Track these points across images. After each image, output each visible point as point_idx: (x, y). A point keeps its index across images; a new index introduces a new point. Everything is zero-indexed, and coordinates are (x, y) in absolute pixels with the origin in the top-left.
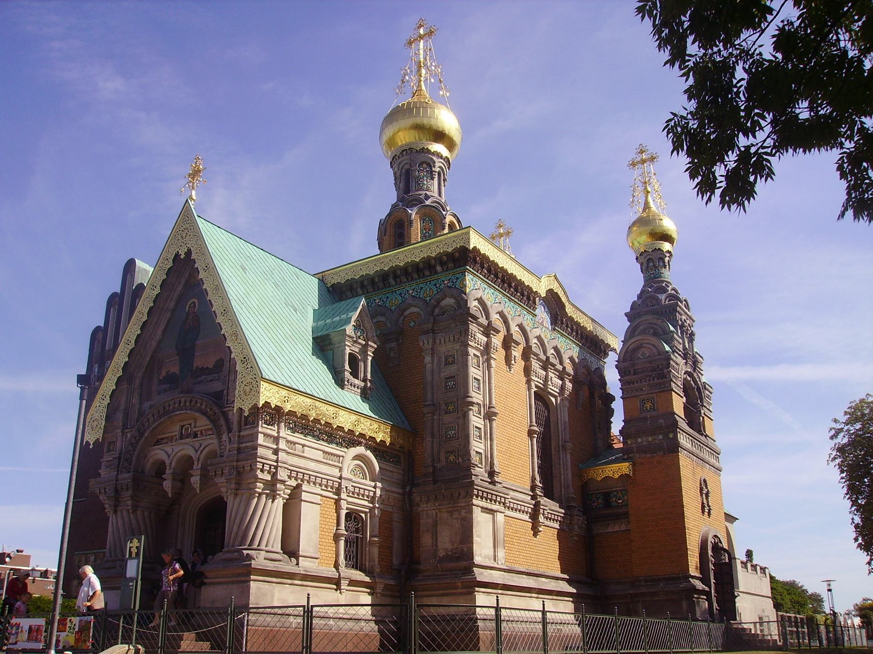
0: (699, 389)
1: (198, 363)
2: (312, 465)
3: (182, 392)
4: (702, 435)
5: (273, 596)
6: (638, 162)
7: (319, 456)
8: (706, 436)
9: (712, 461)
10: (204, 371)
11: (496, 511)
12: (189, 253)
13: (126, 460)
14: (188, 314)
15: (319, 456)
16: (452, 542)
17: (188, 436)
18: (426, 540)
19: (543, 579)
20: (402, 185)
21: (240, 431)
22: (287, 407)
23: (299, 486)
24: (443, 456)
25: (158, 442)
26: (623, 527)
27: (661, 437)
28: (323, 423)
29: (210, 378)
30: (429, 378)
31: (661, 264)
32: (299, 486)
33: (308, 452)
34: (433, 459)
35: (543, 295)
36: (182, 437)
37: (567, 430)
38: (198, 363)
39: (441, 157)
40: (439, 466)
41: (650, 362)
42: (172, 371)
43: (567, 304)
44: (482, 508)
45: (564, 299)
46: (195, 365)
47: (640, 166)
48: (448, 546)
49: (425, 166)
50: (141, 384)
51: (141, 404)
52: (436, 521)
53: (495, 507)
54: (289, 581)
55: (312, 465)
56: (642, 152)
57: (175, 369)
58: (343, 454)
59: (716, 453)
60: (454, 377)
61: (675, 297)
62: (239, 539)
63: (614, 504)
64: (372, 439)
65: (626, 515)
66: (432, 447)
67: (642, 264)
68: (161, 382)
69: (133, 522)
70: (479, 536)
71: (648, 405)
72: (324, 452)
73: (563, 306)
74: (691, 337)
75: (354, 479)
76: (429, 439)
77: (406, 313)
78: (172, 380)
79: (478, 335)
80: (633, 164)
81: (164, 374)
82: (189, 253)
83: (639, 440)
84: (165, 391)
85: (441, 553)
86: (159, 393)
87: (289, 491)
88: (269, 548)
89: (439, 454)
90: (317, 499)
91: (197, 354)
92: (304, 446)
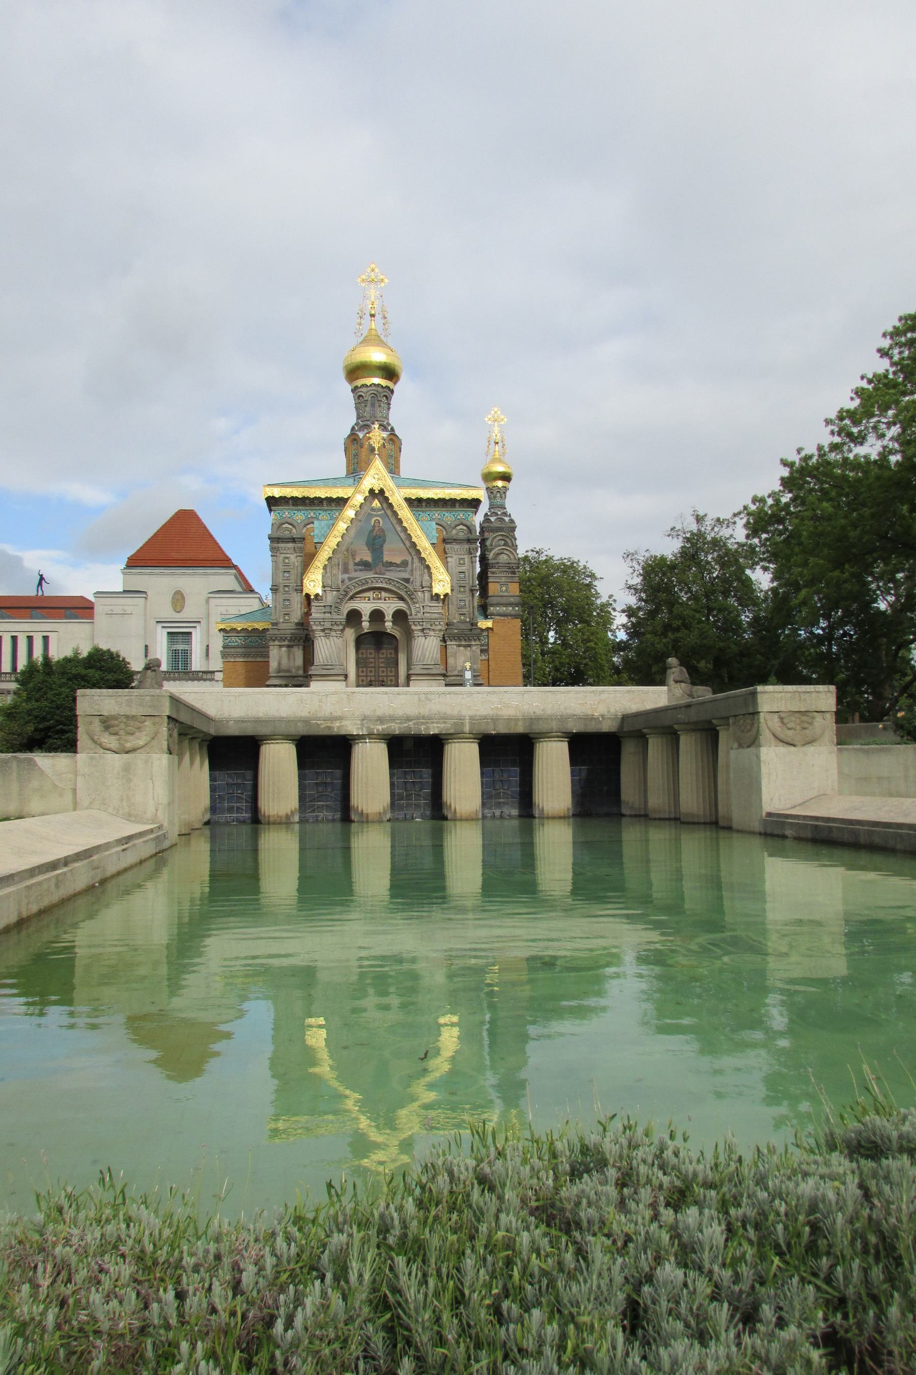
1: (386, 558)
3: (376, 573)
10: (391, 564)
12: (382, 491)
14: (374, 526)
17: (380, 599)
18: (451, 661)
36: (374, 599)
38: (386, 558)
42: (365, 559)
46: (385, 560)
57: (368, 557)
61: (512, 521)
68: (356, 564)
71: (504, 588)
78: (365, 565)
81: (357, 560)
82: (382, 491)
84: (361, 570)
86: (356, 571)
91: (385, 553)
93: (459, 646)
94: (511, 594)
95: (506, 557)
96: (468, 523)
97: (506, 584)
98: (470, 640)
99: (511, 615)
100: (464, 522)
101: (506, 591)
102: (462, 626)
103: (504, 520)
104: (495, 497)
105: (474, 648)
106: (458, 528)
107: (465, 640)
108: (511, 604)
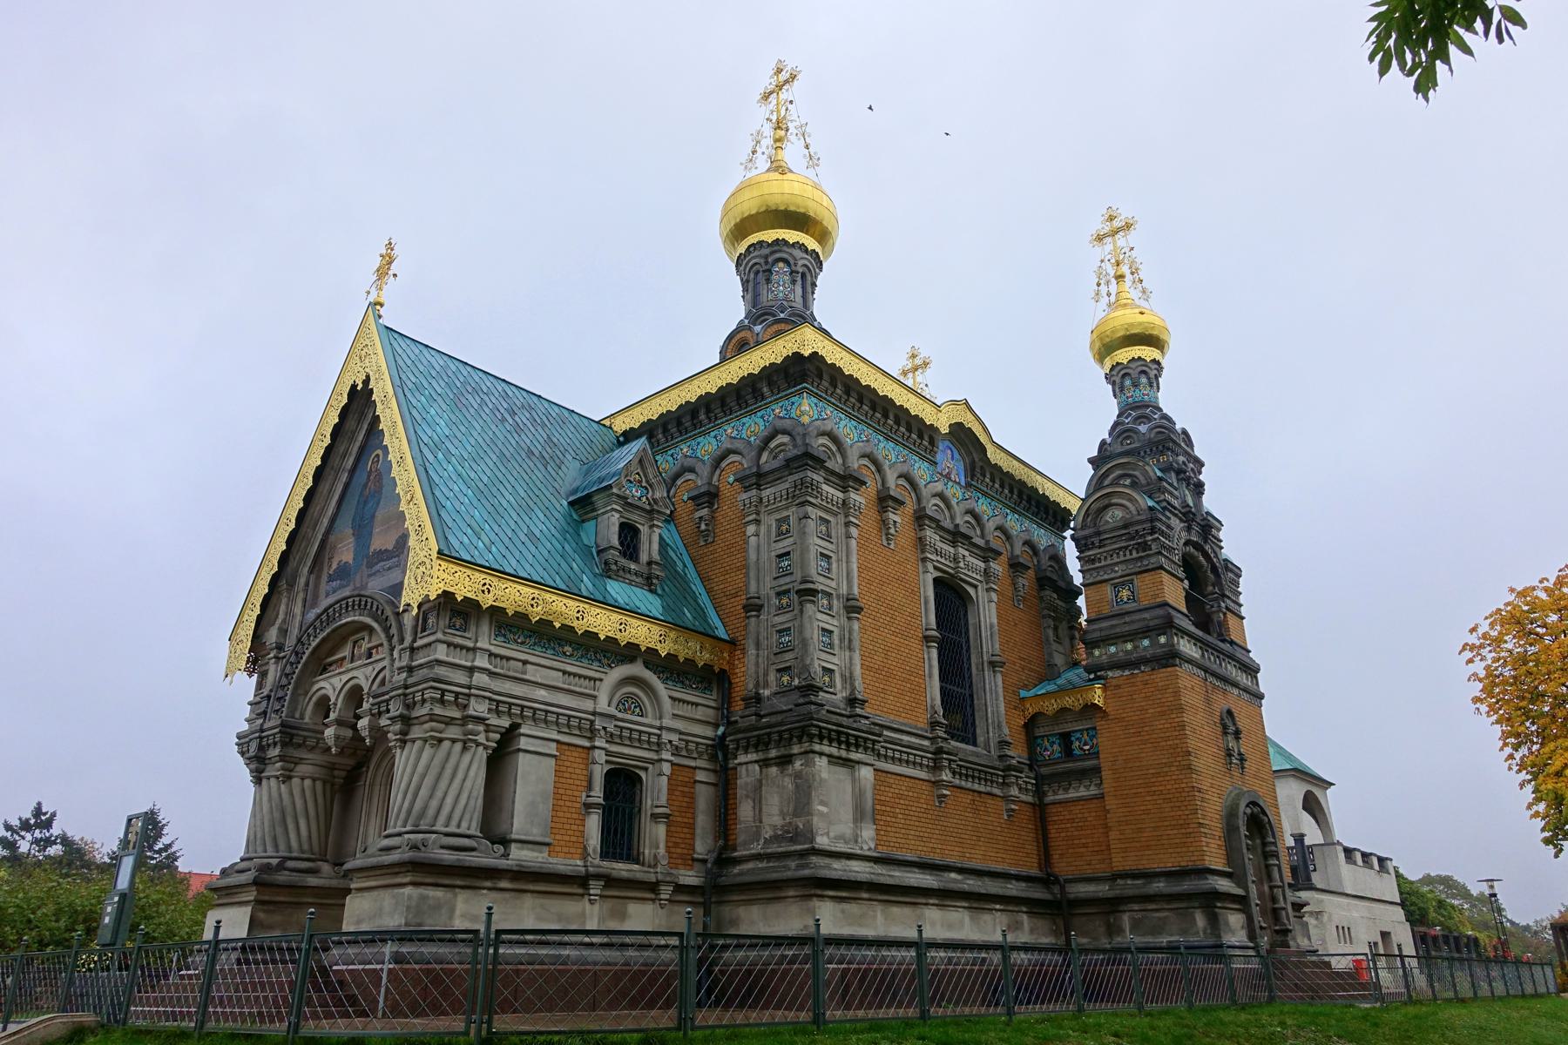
0: (1214, 569)
2: (542, 694)
4: (1223, 641)
5: (452, 910)
6: (1105, 236)
7: (556, 678)
8: (1232, 643)
9: (1243, 679)
11: (858, 763)
12: (367, 381)
13: (279, 699)
15: (556, 678)
16: (783, 814)
18: (745, 811)
19: (953, 875)
20: (749, 297)
21: (414, 641)
22: (487, 601)
23: (515, 727)
24: (772, 677)
25: (324, 670)
26: (1093, 791)
27: (1146, 642)
28: (557, 625)
29: (388, 564)
30: (753, 556)
31: (1144, 380)
32: (515, 727)
33: (532, 673)
34: (757, 685)
35: (945, 430)
37: (996, 638)
39: (806, 251)
40: (767, 693)
41: (1125, 526)
43: (989, 447)
44: (829, 756)
45: (983, 439)
47: (1109, 239)
48: (777, 820)
49: (781, 265)
50: (307, 584)
51: (303, 615)
52: (760, 781)
53: (854, 756)
54: (488, 884)
55: (542, 694)
56: (1111, 218)
58: (597, 675)
59: (1252, 670)
60: (788, 553)
62: (402, 816)
63: (1077, 752)
64: (652, 652)
65: (1097, 770)
66: (757, 664)
67: (1113, 384)
69: (285, 796)
70: (823, 803)
71: (1125, 593)
72: (564, 672)
73: (984, 450)
74: (1199, 488)
75: (620, 715)
76: (752, 651)
77: (723, 465)
79: (825, 487)
80: (1100, 238)
81: (334, 566)
83: (1113, 649)
85: (767, 833)
87: (498, 736)
88: (452, 829)
89: (766, 674)
90: (552, 748)
92: (525, 662)
93: (765, 763)
94: (1145, 603)
95: (1119, 513)
96: (787, 424)
97: (1125, 581)
98: (790, 744)
99: (1144, 661)
100: (780, 424)
101: (1133, 598)
102: (782, 704)
103: (1136, 432)
104: (1122, 389)
105: (798, 764)
106: (772, 445)
107: (778, 744)
108: (1146, 632)
